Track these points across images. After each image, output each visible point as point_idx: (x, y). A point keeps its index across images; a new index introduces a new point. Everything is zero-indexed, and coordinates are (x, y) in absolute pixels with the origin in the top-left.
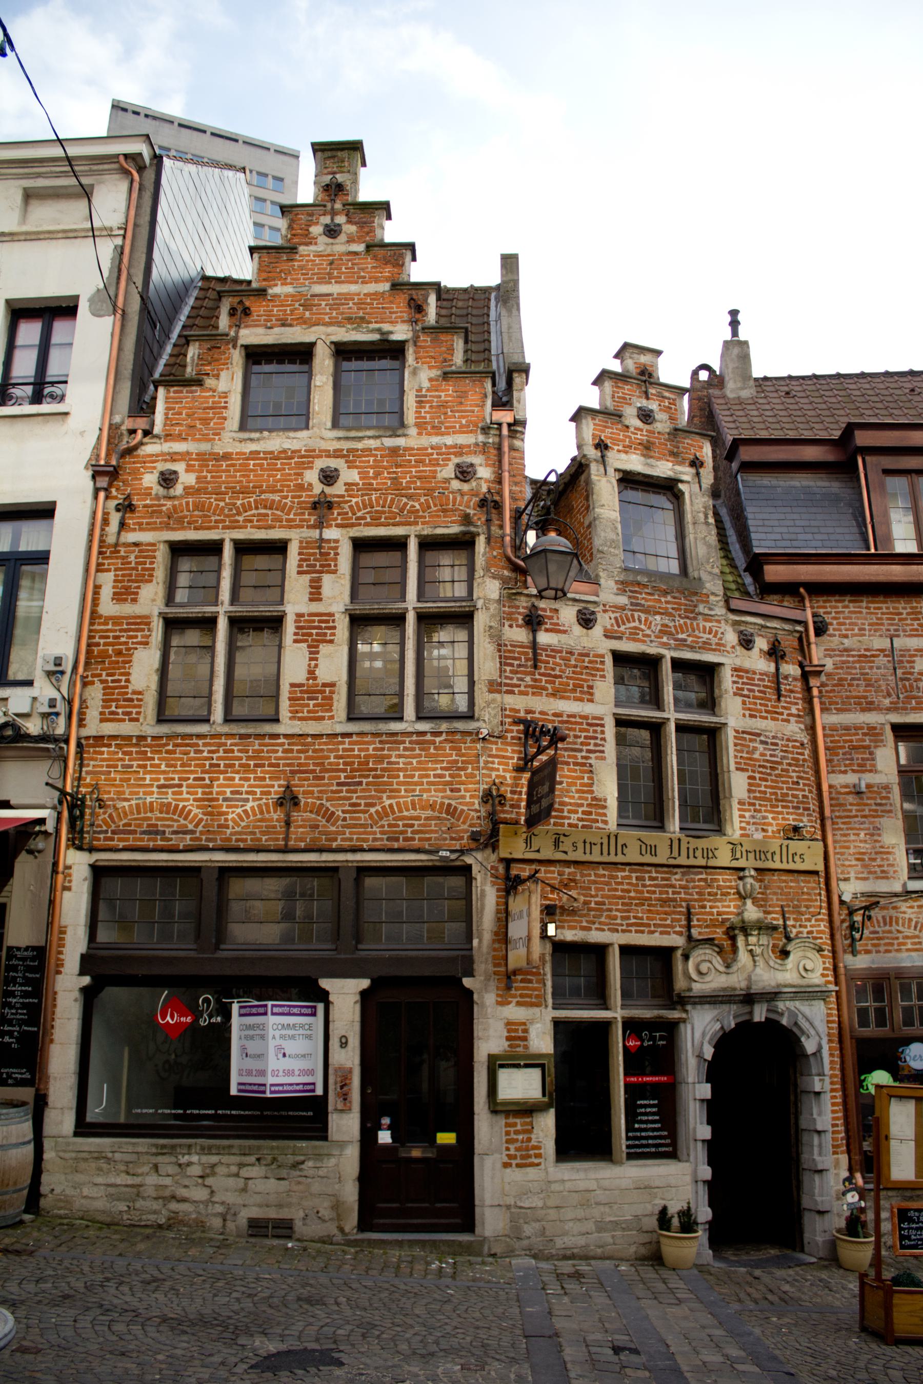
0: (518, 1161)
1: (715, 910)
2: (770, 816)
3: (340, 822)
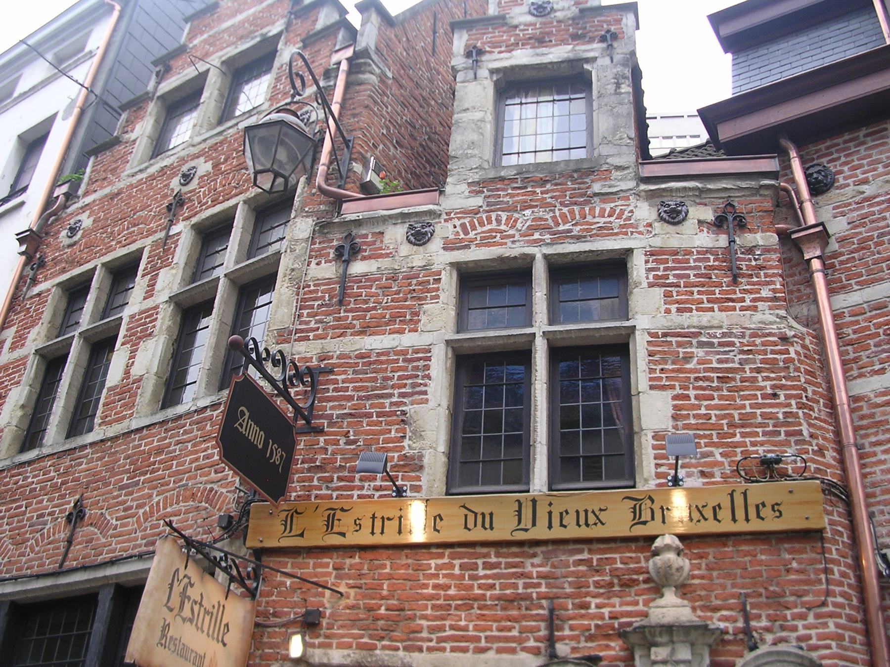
1: (606, 611)
2: (717, 452)
3: (111, 532)
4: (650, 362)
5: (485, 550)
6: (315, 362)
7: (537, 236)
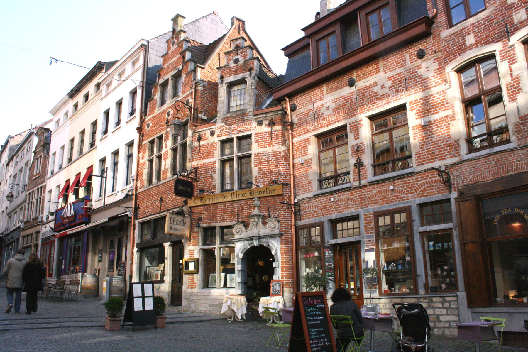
2: (266, 179)
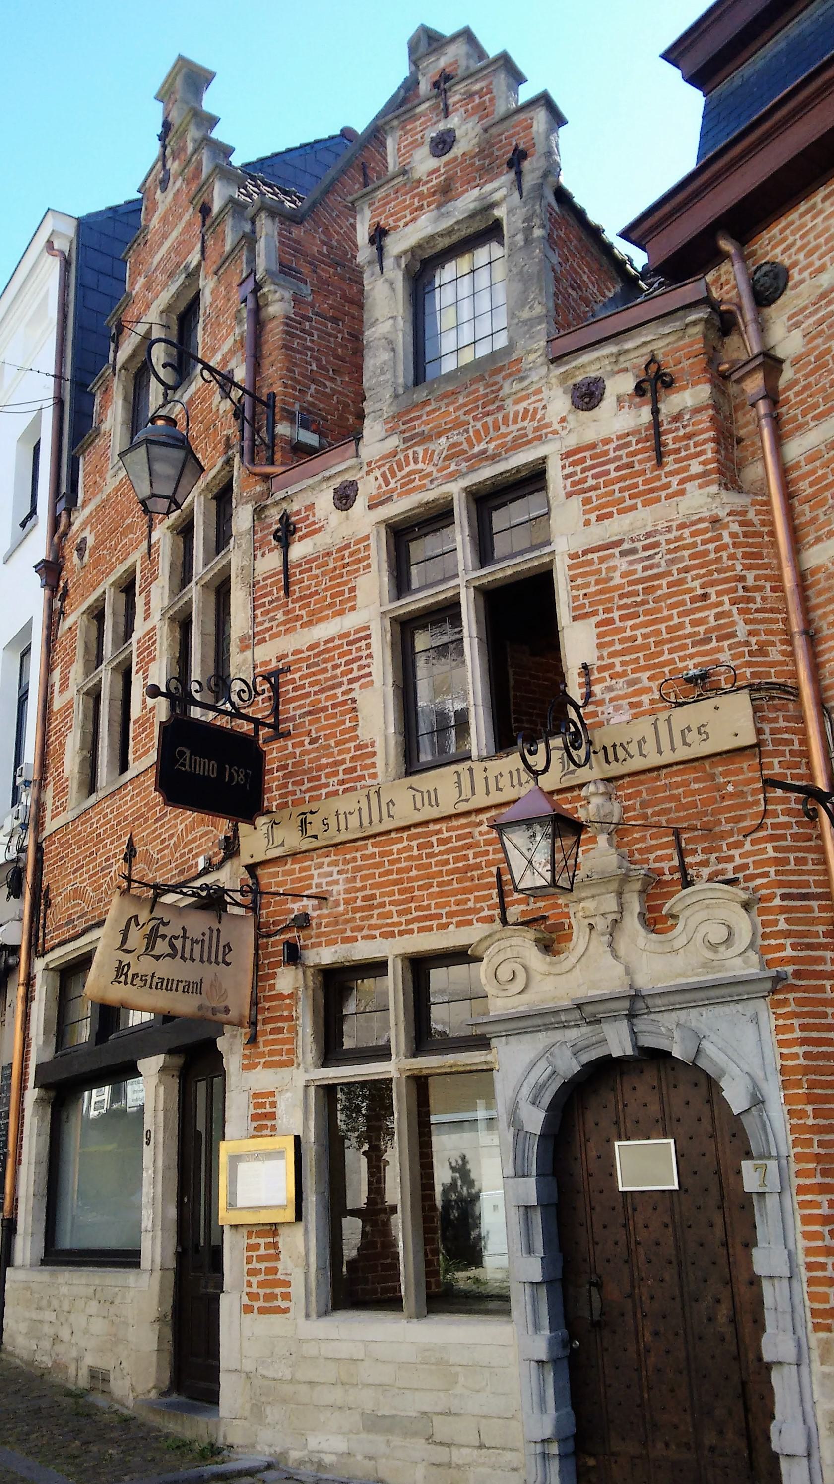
0: (261, 1303)
4: (572, 588)
5: (437, 827)
6: (274, 664)
7: (453, 467)
